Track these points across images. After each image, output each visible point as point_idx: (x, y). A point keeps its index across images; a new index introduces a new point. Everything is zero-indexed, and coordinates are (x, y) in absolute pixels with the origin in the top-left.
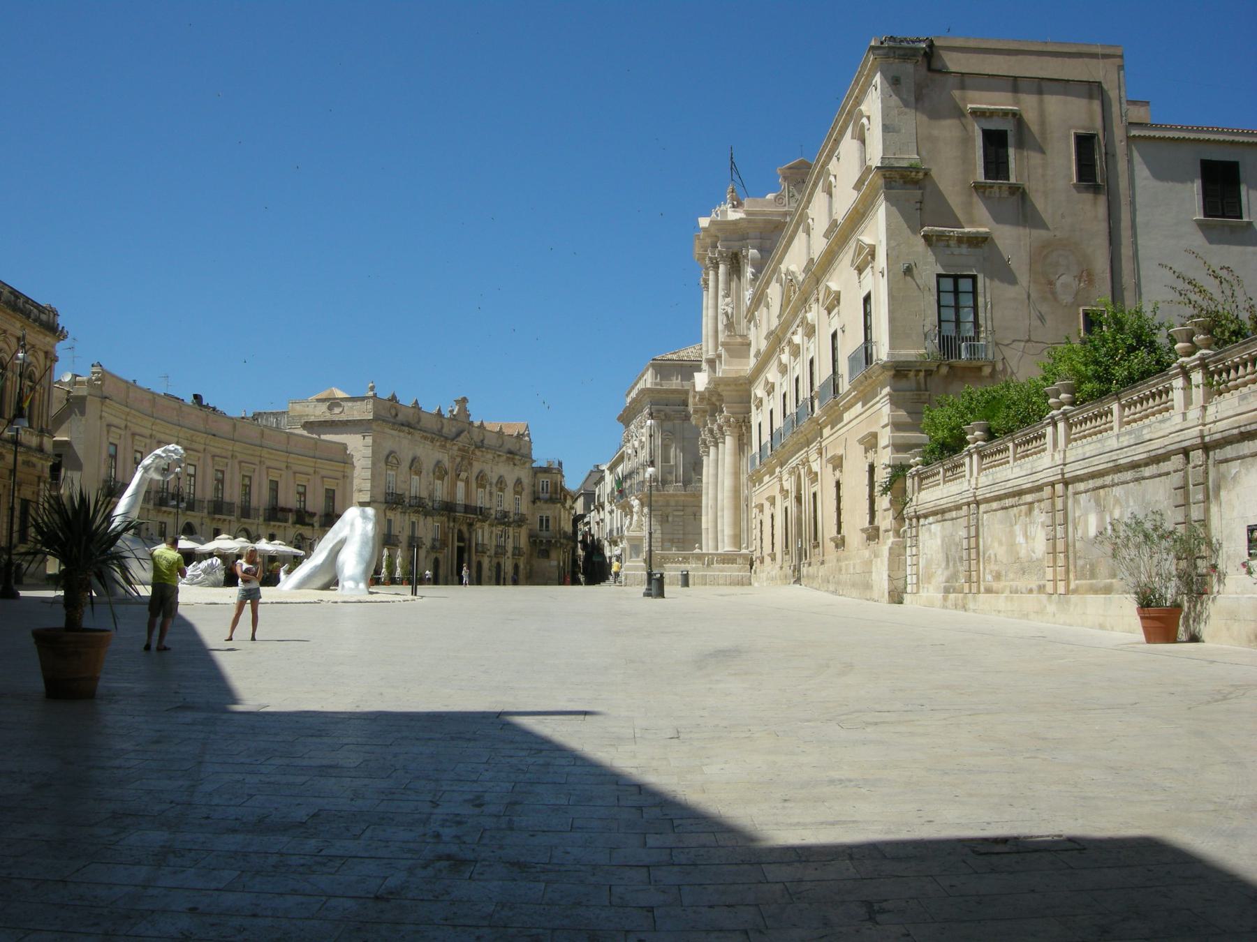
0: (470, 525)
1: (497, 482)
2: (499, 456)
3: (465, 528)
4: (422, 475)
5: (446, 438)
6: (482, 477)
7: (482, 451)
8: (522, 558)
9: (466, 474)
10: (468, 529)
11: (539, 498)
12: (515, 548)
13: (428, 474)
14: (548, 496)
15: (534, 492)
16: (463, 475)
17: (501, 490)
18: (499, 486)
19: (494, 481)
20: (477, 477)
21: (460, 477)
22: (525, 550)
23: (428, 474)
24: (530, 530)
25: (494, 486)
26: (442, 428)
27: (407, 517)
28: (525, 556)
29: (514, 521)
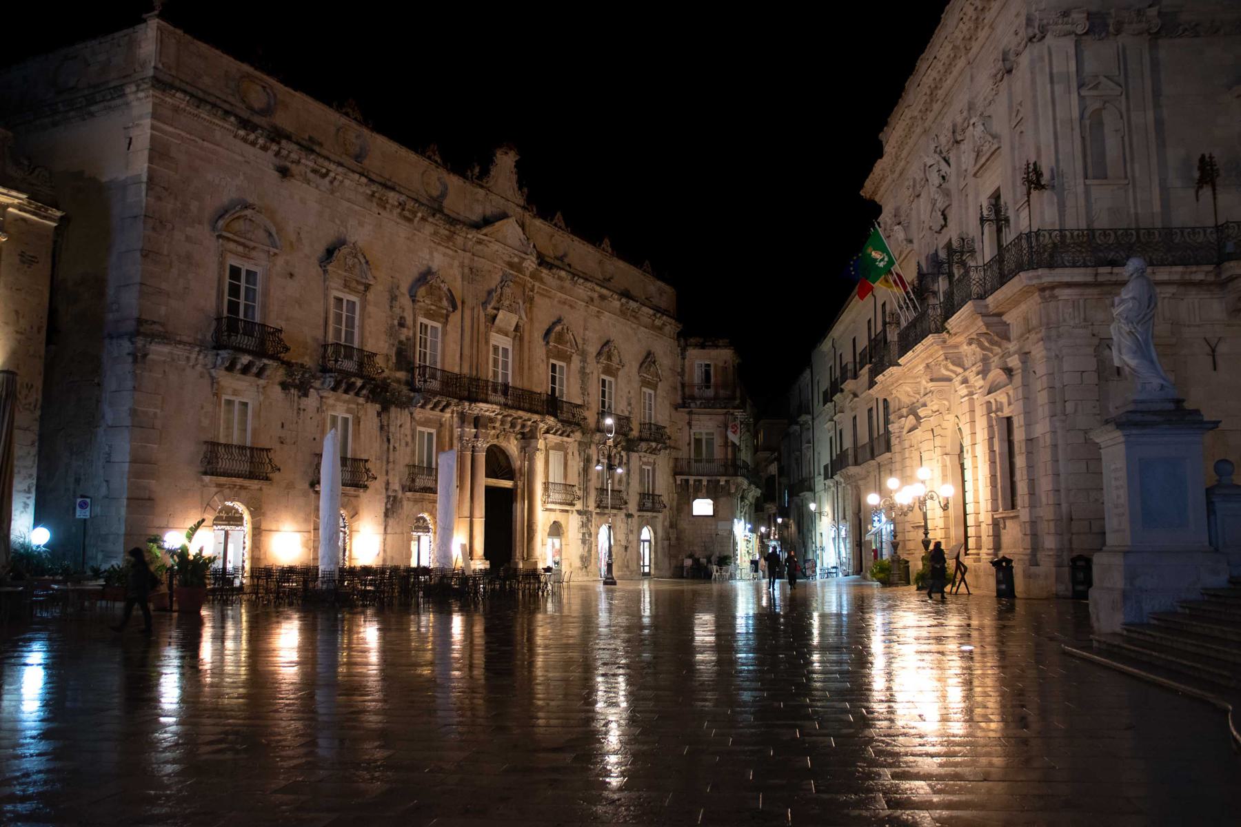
0: (527, 438)
1: (599, 354)
2: (602, 297)
3: (512, 447)
4: (370, 296)
5: (452, 221)
6: (560, 335)
7: (560, 278)
8: (660, 516)
9: (514, 319)
10: (523, 449)
11: (693, 398)
12: (643, 496)
13: (393, 298)
14: (710, 393)
15: (683, 385)
16: (506, 319)
17: (608, 371)
18: (603, 360)
19: (593, 350)
20: (548, 333)
21: (497, 321)
22: (665, 499)
23: (393, 298)
24: (676, 459)
25: (591, 359)
26: (444, 195)
27: (311, 401)
28: (666, 511)
29: (641, 439)
